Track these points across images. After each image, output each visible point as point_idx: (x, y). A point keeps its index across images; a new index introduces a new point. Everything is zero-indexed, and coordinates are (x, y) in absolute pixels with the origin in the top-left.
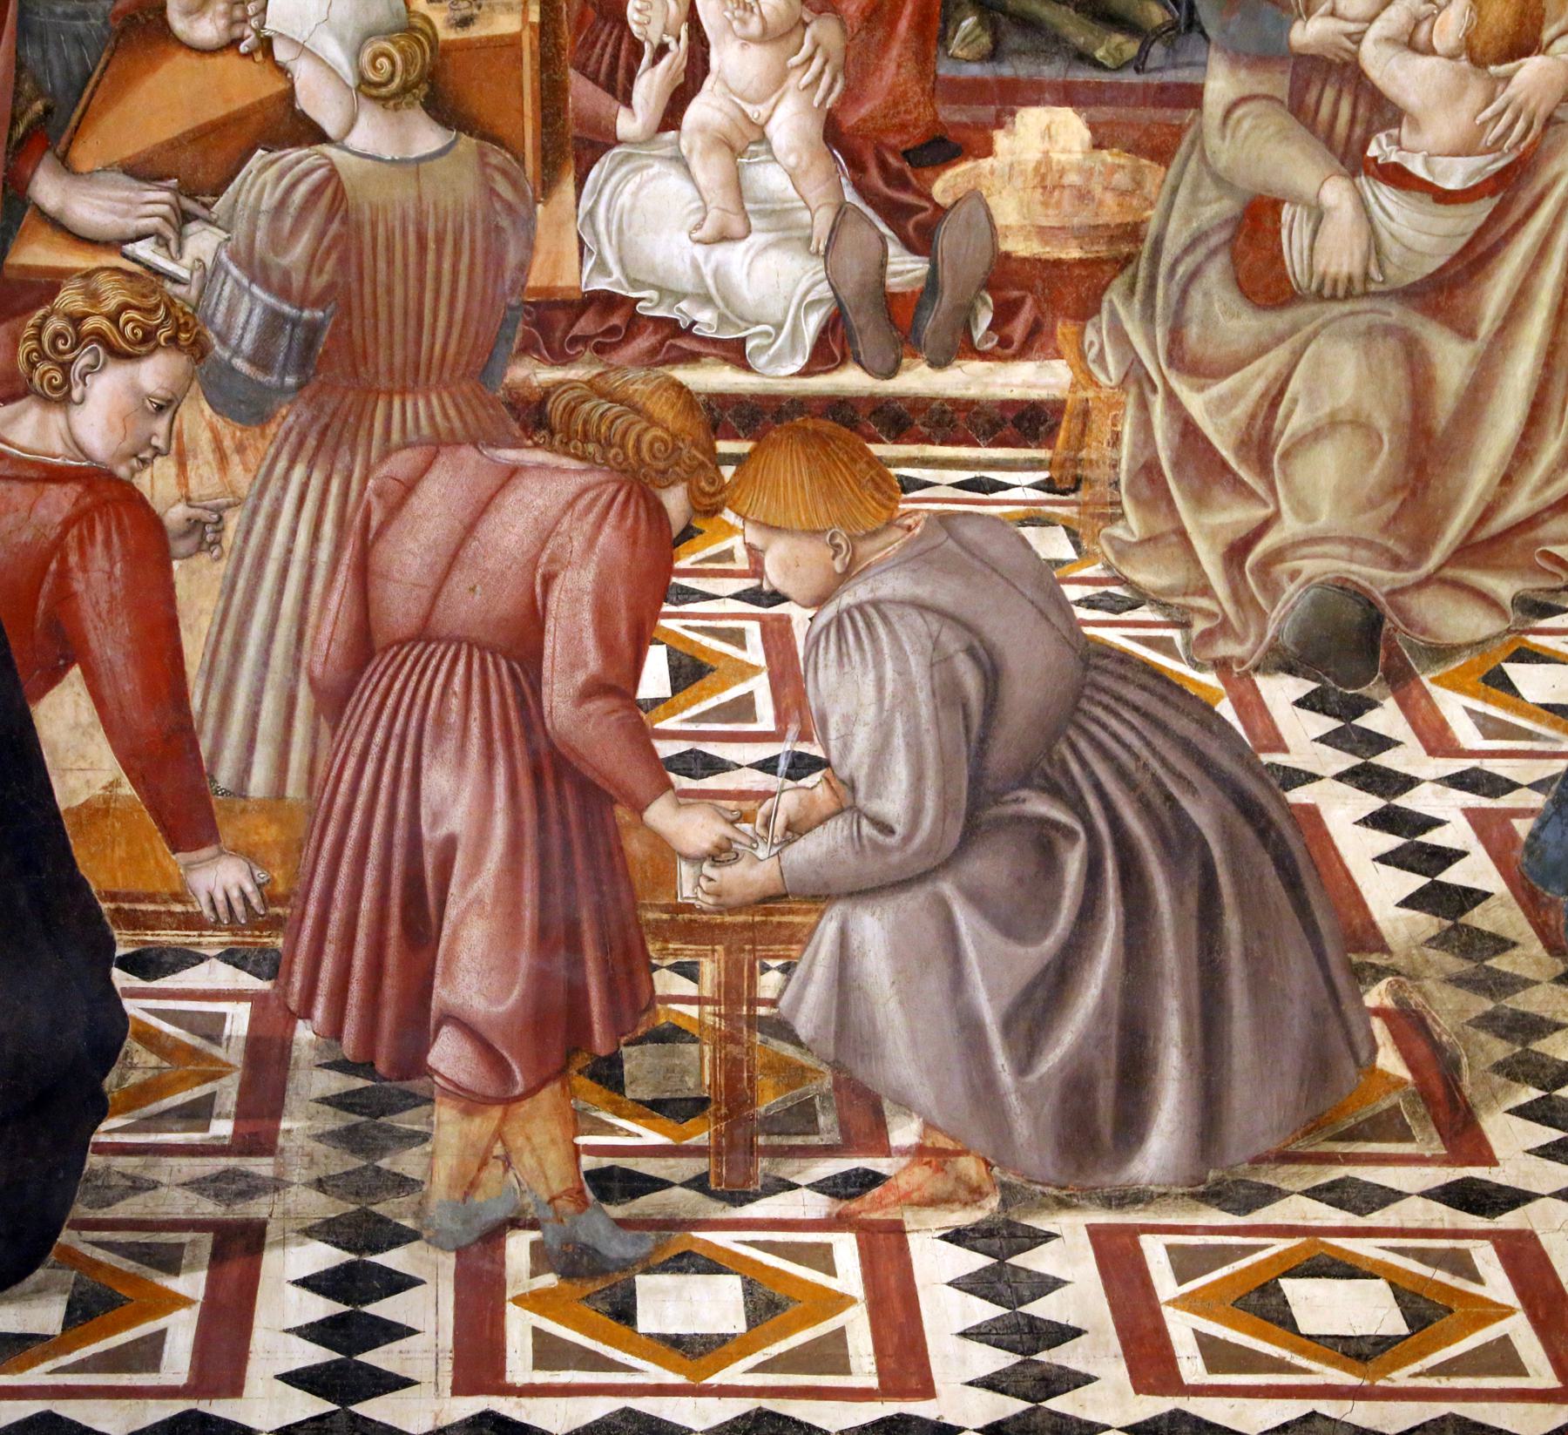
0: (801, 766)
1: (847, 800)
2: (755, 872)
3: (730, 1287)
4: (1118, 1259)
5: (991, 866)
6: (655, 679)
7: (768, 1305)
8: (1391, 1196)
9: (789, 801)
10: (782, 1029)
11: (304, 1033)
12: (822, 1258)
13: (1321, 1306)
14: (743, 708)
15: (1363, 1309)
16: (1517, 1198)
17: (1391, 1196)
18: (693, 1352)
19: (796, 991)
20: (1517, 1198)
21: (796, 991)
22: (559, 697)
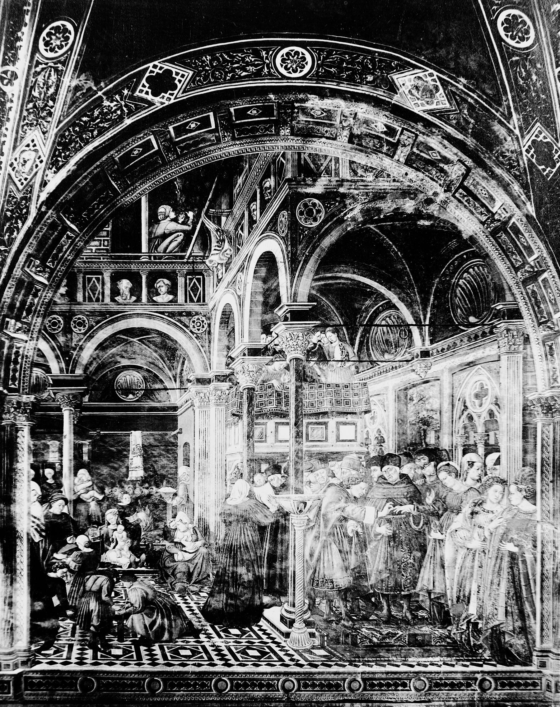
0: (128, 603)
1: (132, 605)
2: (123, 612)
3: (121, 650)
4: (161, 648)
5: (147, 611)
6: (113, 594)
7: (125, 652)
8: (189, 642)
9: (127, 605)
10: (126, 626)
11: (78, 626)
12: (131, 648)
13: (183, 652)
14: (122, 597)
15: (188, 653)
16: (203, 642)
17: (189, 642)
18: (117, 657)
19: (128, 623)
20: (203, 642)
21: (128, 623)
22: (104, 597)
